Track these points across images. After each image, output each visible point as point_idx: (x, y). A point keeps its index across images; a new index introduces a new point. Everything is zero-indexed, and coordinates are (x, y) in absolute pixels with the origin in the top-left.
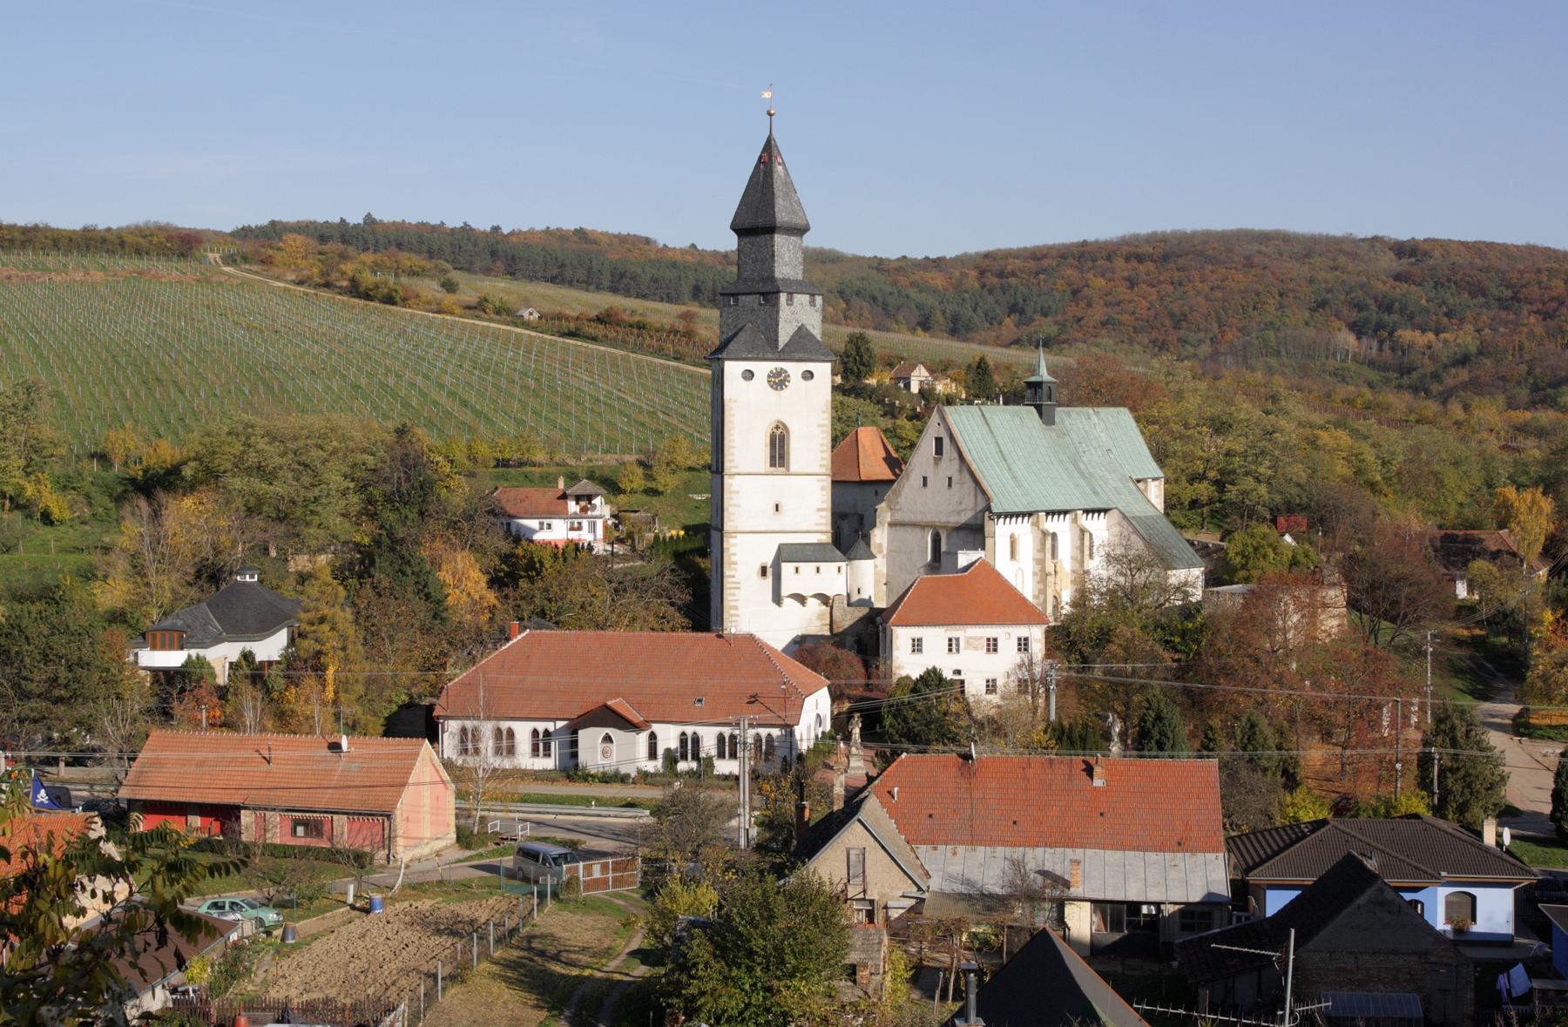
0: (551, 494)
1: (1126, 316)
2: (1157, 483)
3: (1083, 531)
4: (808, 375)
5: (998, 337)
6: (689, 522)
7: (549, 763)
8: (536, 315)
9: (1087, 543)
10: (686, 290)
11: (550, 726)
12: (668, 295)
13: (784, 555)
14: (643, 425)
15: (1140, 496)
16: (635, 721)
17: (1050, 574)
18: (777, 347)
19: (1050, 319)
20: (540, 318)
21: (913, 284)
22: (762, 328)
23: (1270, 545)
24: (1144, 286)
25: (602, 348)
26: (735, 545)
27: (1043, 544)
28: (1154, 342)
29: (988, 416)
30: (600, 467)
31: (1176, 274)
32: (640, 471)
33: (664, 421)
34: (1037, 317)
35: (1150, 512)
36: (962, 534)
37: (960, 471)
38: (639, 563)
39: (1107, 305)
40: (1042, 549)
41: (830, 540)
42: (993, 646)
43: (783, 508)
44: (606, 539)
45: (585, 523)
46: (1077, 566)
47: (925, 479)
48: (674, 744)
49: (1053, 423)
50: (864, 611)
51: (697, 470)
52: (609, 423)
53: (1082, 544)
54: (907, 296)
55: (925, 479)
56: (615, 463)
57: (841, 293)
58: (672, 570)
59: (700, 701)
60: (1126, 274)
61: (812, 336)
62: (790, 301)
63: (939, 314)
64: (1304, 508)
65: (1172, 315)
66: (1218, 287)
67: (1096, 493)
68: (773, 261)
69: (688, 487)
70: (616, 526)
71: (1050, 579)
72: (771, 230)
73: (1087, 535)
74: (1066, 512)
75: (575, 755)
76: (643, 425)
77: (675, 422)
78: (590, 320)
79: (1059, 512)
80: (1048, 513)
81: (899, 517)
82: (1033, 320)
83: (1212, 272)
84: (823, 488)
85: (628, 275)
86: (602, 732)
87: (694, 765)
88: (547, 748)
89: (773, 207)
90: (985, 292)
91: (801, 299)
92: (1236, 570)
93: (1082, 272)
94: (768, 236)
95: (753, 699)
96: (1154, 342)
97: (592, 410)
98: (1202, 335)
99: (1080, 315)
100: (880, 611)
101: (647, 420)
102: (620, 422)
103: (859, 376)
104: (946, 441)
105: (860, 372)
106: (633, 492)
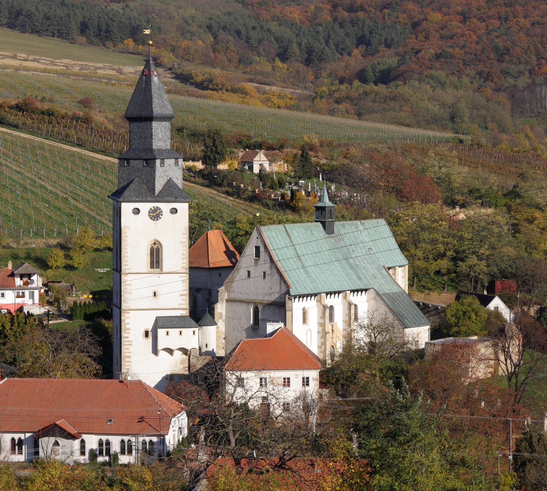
1: (457, 50)
2: (403, 268)
3: (350, 304)
4: (174, 211)
5: (346, 67)
6: (95, 290)
7: (21, 458)
9: (353, 311)
10: (75, 27)
11: (22, 436)
12: (59, 31)
13: (160, 324)
14: (60, 209)
15: (389, 279)
16: (73, 433)
17: (328, 333)
18: (154, 194)
19: (392, 51)
21: (274, 18)
22: (145, 181)
23: (473, 310)
24: (475, 20)
25: (22, 135)
26: (129, 318)
27: (324, 314)
28: (480, 74)
29: (289, 231)
30: (34, 249)
31: (503, 9)
32: (61, 253)
33: (74, 206)
34: (382, 48)
35: (395, 289)
36: (272, 308)
37: (271, 268)
38: (64, 320)
39: (442, 38)
40: (323, 317)
41: (188, 314)
42: (287, 382)
44: (43, 301)
45: (27, 293)
46: (347, 327)
47: (249, 272)
48: (95, 446)
49: (333, 233)
50: (208, 358)
51: (101, 251)
52: (36, 209)
53: (350, 312)
54: (269, 30)
55: (249, 272)
56: (42, 245)
57: (209, 27)
58: (90, 336)
59: (110, 421)
60: (460, 9)
61: (177, 185)
62: (162, 163)
63: (295, 46)
64: (514, 276)
65: (496, 49)
66: (538, 23)
68: (152, 138)
69: (94, 263)
70: (46, 292)
71: (329, 336)
72: (150, 119)
73: (353, 307)
74: (339, 293)
75: (37, 453)
76: (60, 209)
77: (81, 206)
78: (11, 108)
79: (335, 293)
80: (327, 294)
81: (233, 296)
82: (378, 51)
83: (534, 8)
85: (24, 13)
86: (52, 440)
87: (107, 458)
88: (20, 449)
89: (152, 105)
90: (337, 26)
91: (169, 162)
92: (451, 326)
93: (422, 7)
94: (148, 123)
95: (141, 420)
96: (480, 74)
97: (22, 198)
98: (522, 67)
99: (417, 47)
100: (220, 358)
101: (62, 205)
102: (41, 205)
103: (215, 163)
104: (262, 249)
105: (215, 159)
106: (57, 267)
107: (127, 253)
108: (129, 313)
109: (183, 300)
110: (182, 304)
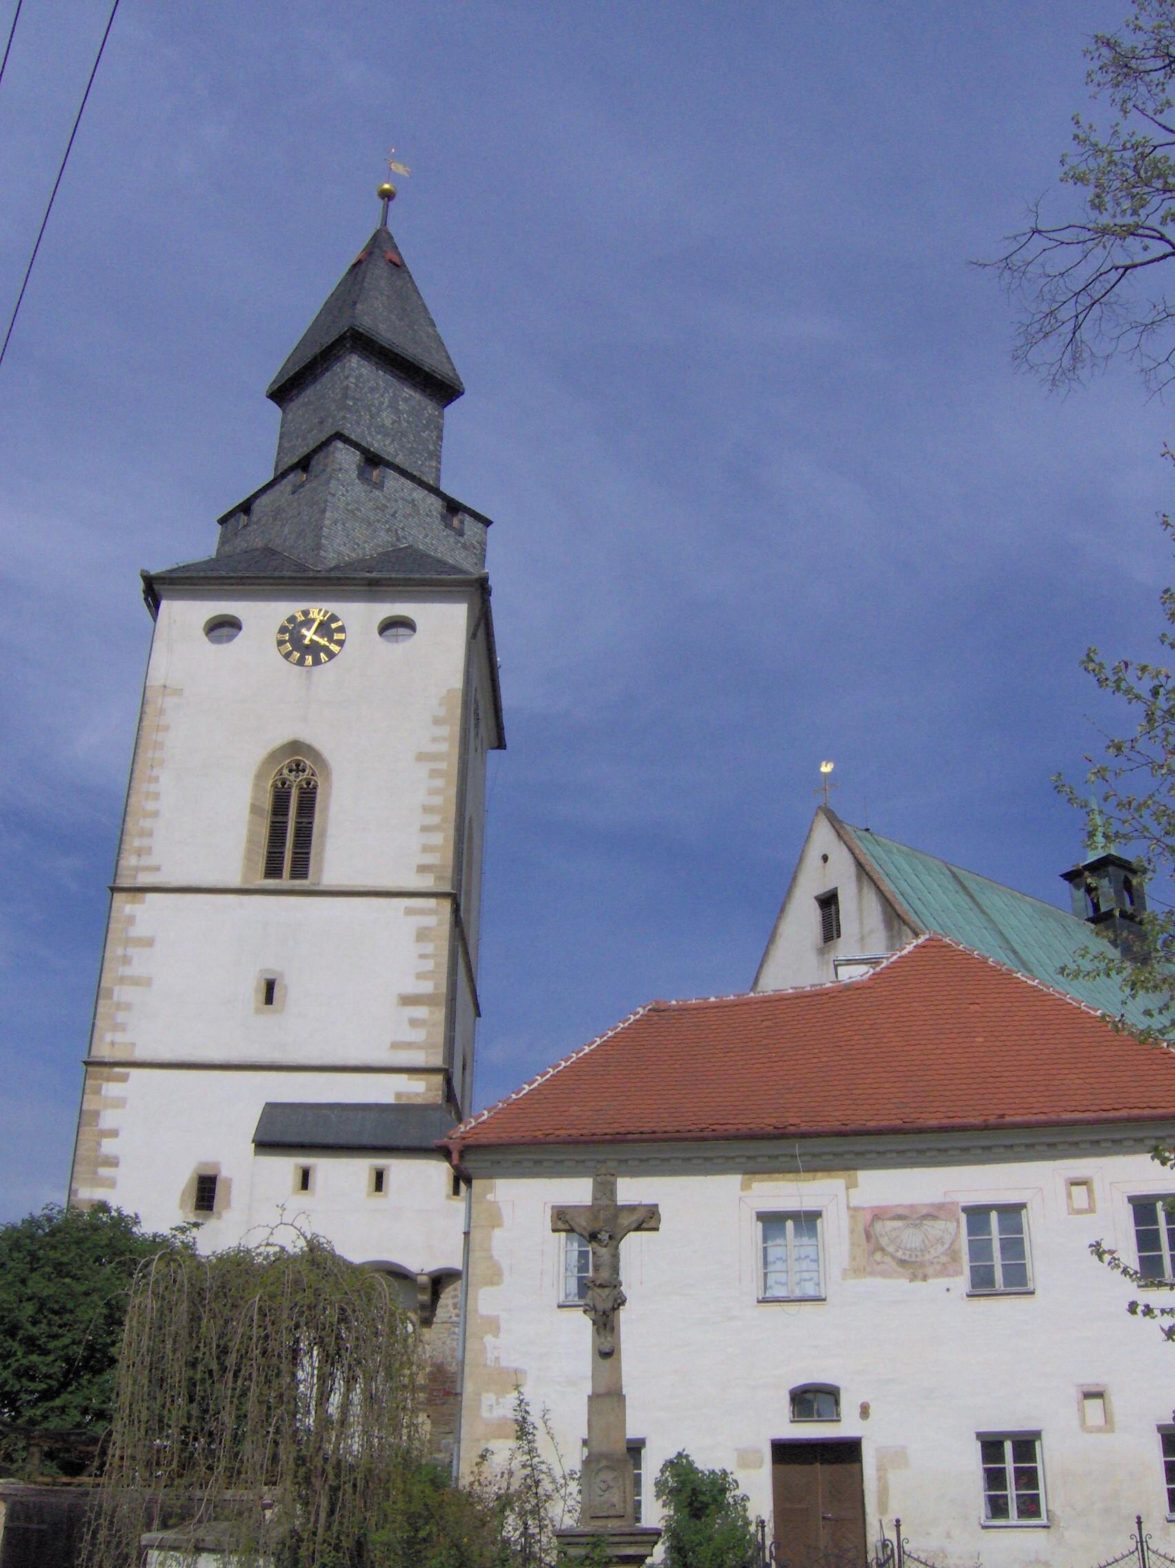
26: (120, 1103)
43: (292, 991)
84: (422, 935)
107: (157, 796)
108: (124, 1079)
109: (414, 1023)
110: (409, 1045)
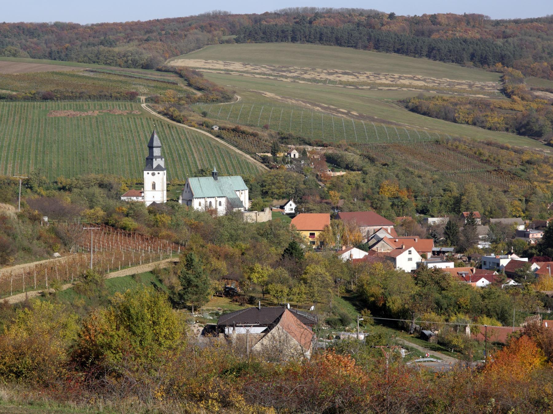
0: (139, 191)
4: (159, 173)
8: (218, 128)
20: (219, 129)
62: (156, 160)
67: (222, 193)
91: (159, 160)
